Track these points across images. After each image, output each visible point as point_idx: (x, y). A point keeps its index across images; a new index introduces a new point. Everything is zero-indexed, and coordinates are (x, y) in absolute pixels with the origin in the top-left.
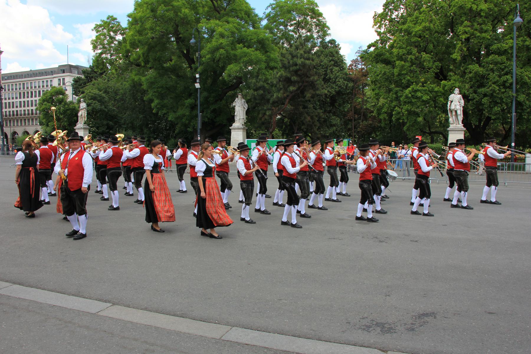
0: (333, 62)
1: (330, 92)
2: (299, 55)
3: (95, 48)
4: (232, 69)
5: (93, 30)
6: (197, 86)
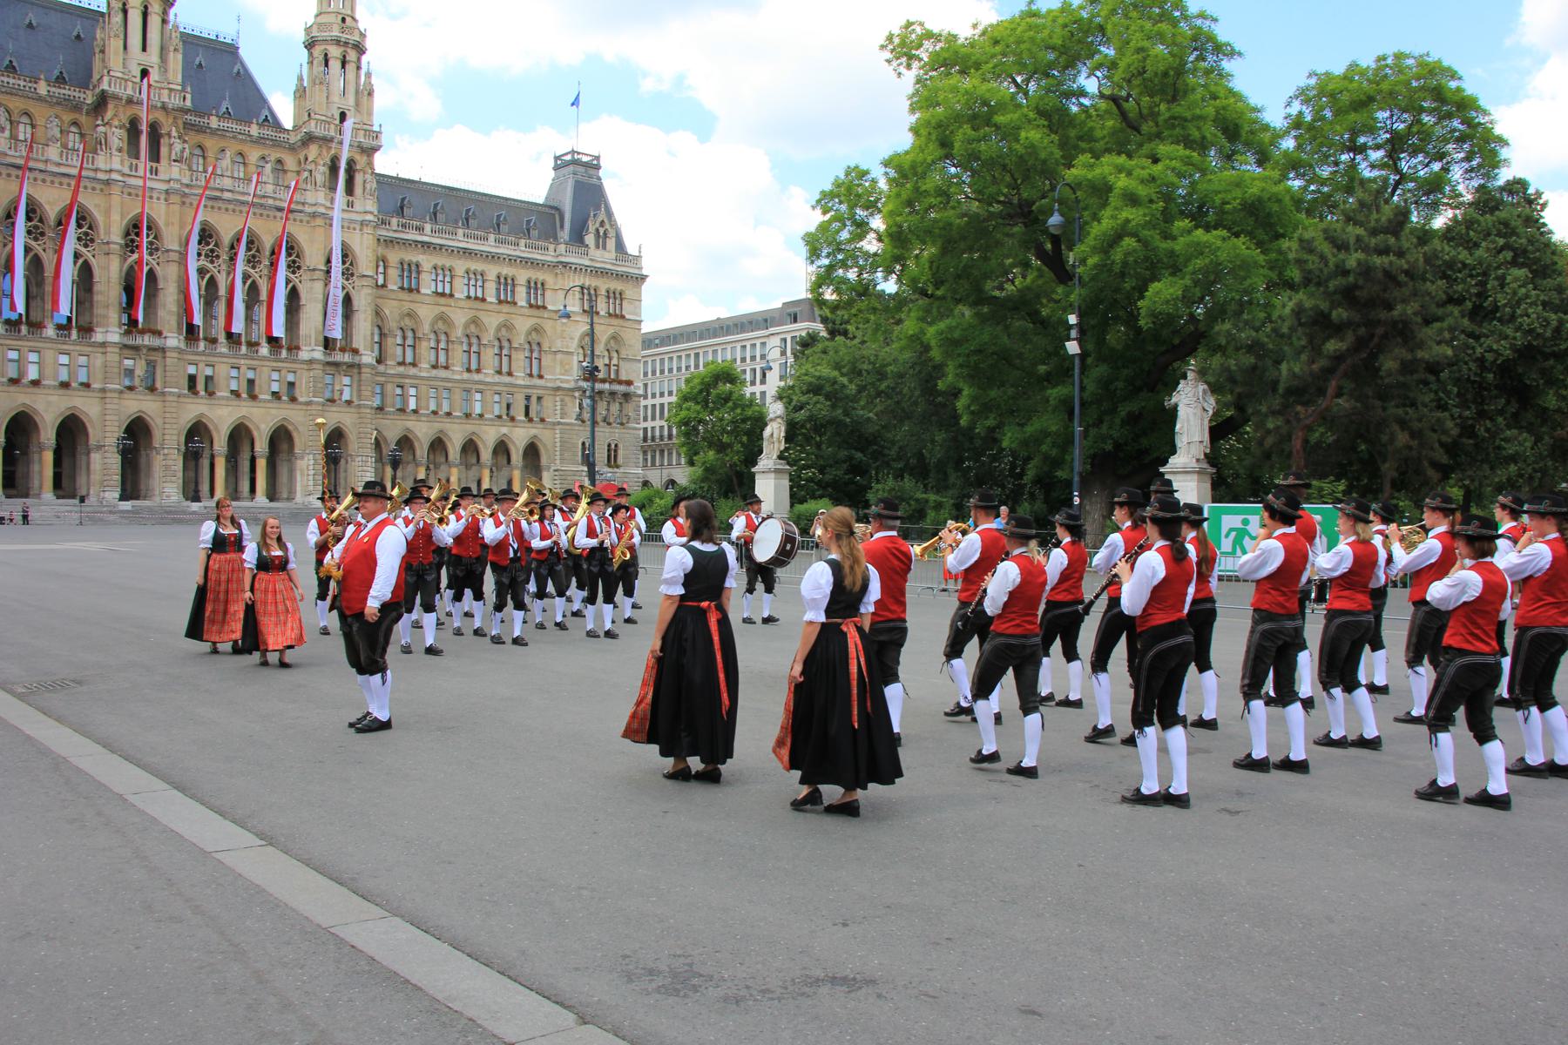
0: (1509, 255)
1: (1496, 352)
2: (1352, 241)
3: (814, 254)
4: (1162, 292)
5: (813, 207)
6: (1073, 347)
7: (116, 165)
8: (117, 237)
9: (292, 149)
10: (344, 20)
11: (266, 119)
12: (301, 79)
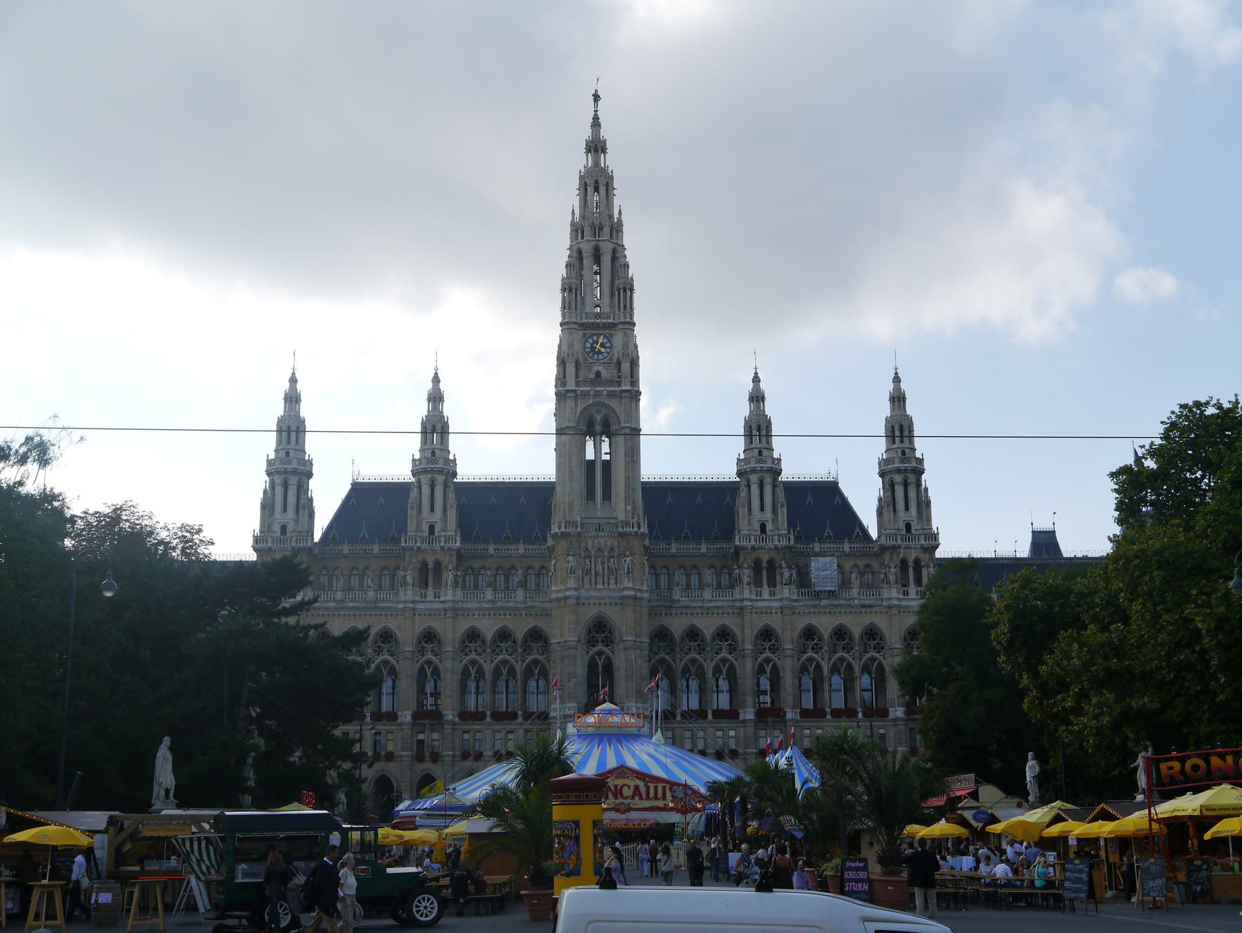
7: (746, 595)
8: (748, 646)
9: (876, 555)
10: (903, 453)
11: (858, 535)
12: (880, 500)
